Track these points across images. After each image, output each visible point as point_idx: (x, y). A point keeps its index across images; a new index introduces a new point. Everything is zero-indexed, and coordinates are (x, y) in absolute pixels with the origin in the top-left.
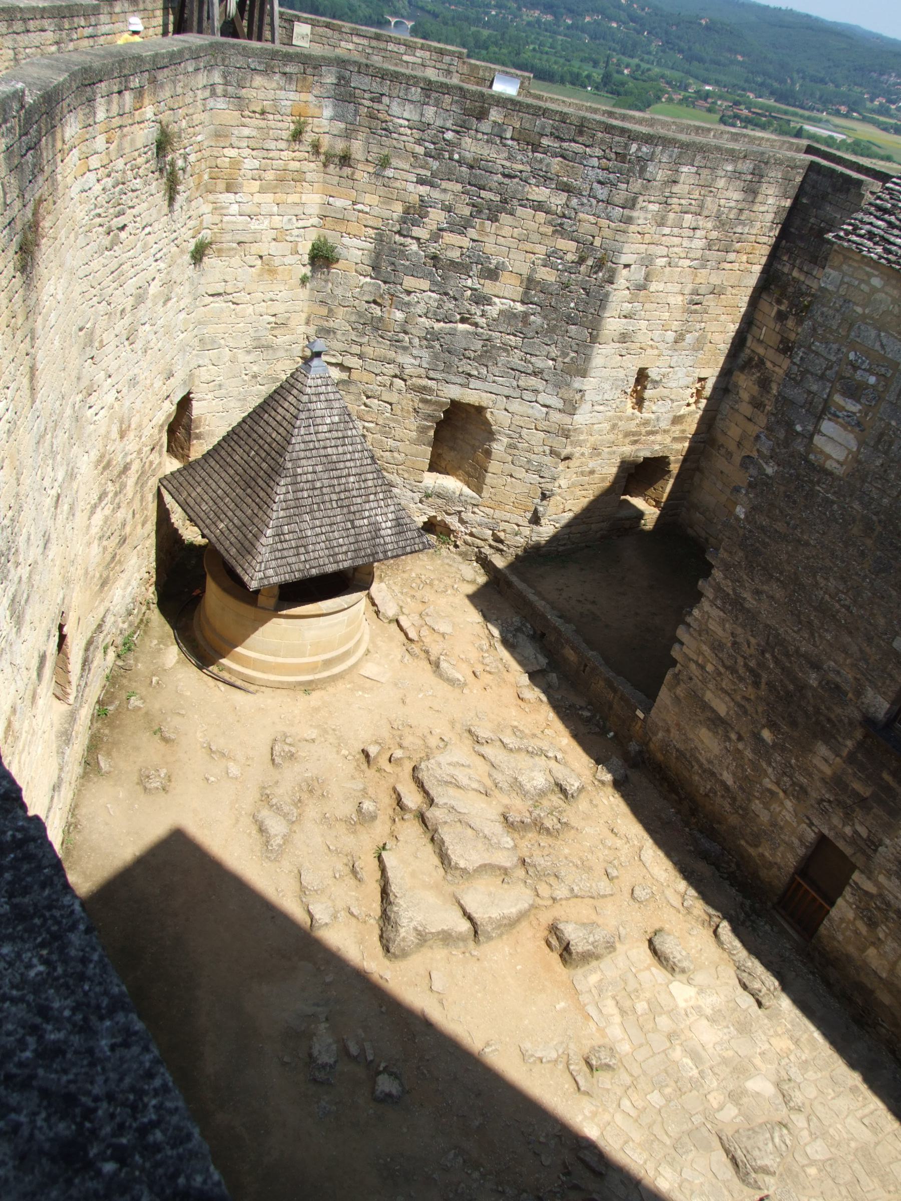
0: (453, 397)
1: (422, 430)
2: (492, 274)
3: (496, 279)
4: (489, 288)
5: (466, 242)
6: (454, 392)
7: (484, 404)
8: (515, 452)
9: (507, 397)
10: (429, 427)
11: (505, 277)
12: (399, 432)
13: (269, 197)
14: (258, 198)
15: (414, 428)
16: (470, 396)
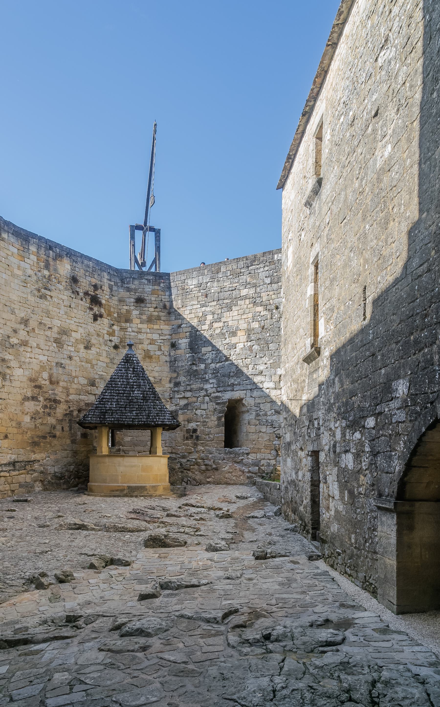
0: (228, 398)
1: (219, 419)
2: (234, 334)
3: (236, 336)
4: (234, 340)
5: (221, 324)
6: (228, 396)
7: (242, 397)
8: (260, 418)
9: (251, 390)
10: (222, 416)
11: (239, 333)
12: (210, 424)
13: (145, 326)
14: (140, 326)
15: (215, 419)
16: (236, 395)
